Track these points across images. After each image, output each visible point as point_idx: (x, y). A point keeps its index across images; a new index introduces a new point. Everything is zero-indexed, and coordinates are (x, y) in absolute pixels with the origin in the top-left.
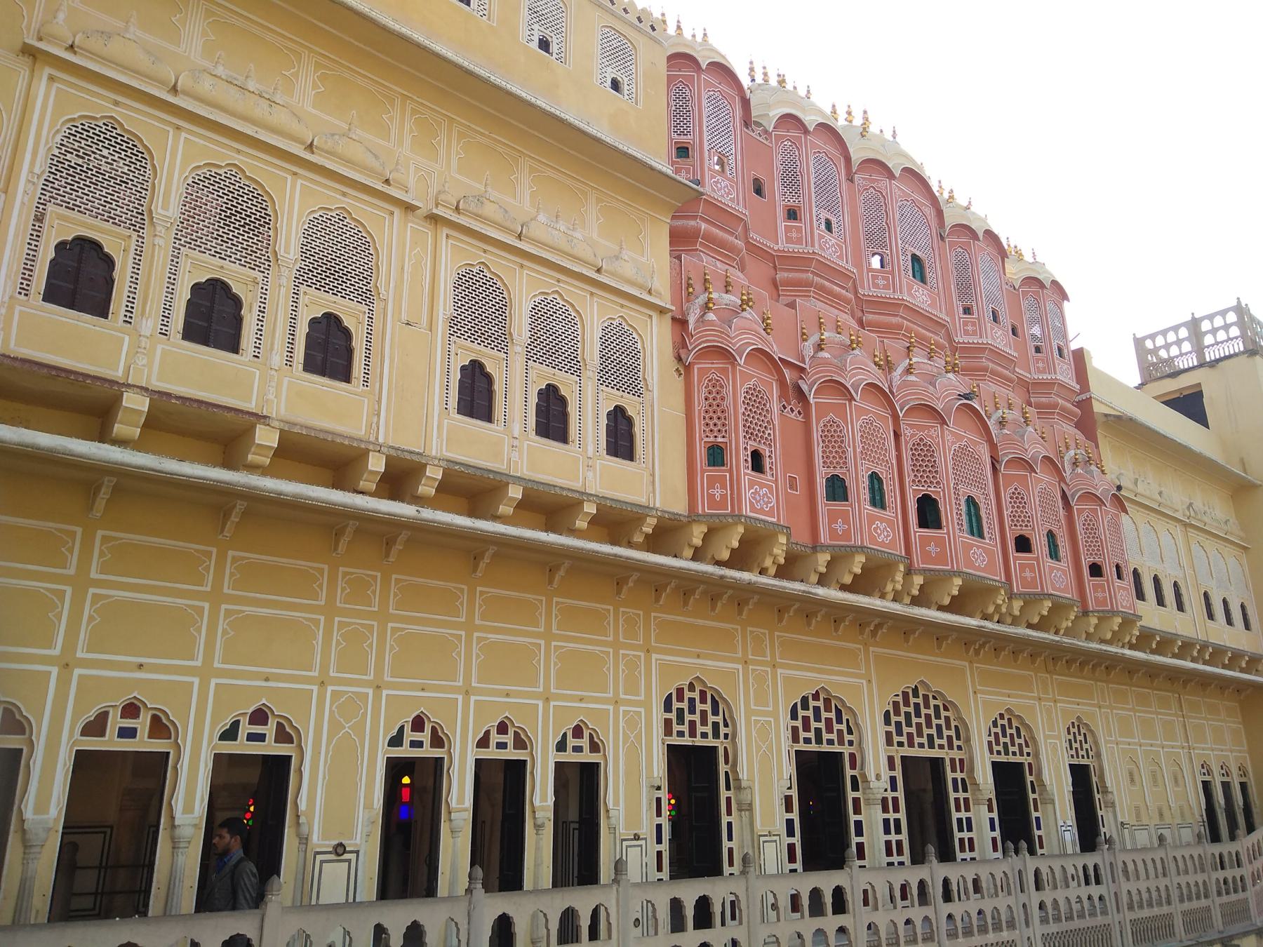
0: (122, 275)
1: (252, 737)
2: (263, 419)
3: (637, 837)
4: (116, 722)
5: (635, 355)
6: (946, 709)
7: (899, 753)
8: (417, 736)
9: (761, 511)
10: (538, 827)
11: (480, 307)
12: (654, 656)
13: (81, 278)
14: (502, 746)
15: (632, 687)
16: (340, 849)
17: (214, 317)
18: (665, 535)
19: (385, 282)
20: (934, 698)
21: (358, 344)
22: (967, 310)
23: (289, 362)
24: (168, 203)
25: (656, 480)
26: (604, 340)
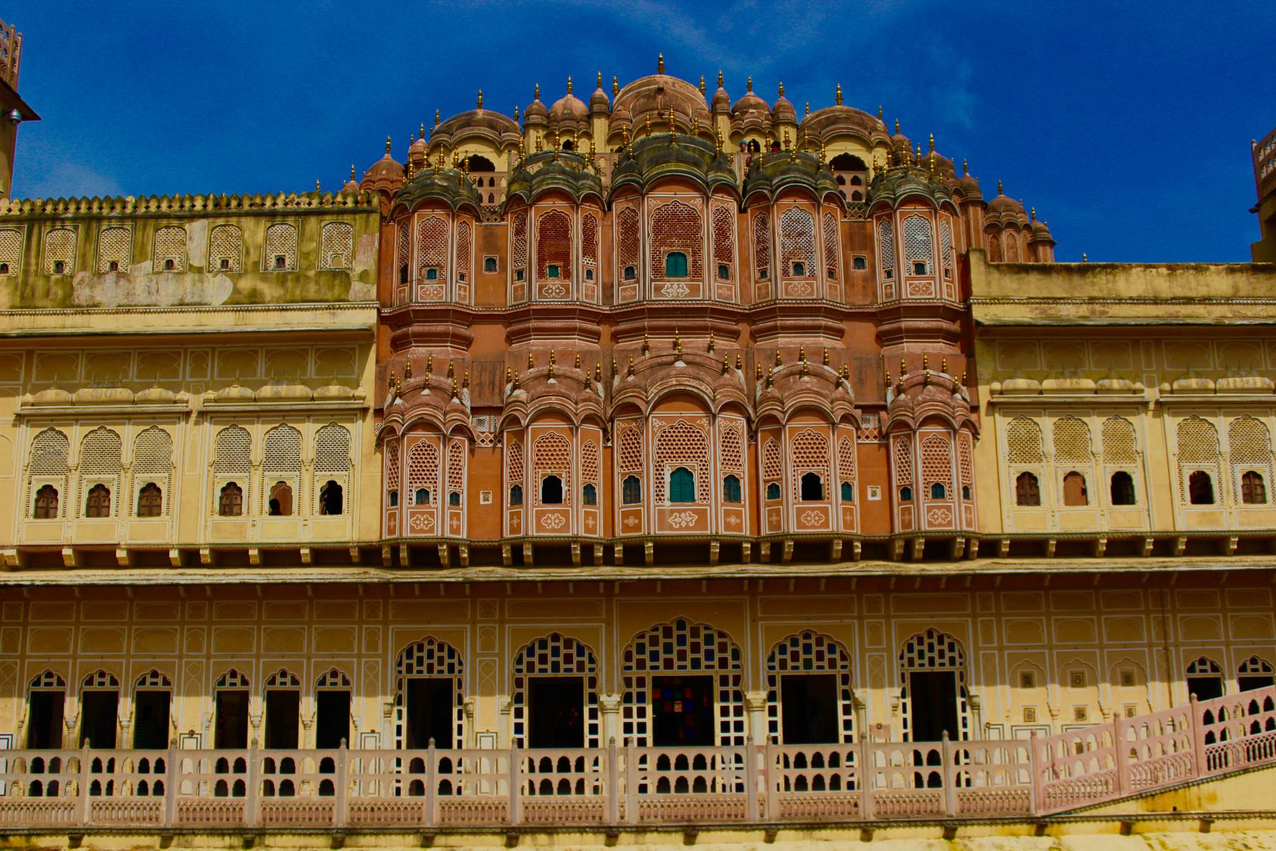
0: (60, 497)
1: (152, 684)
2: (117, 545)
4: (97, 679)
6: (721, 635)
7: (648, 674)
8: (233, 680)
9: (422, 531)
10: (305, 726)
13: (46, 502)
14: (284, 683)
15: (372, 646)
16: (192, 733)
17: (98, 501)
18: (369, 555)
19: (173, 459)
20: (707, 628)
22: (763, 274)
23: (130, 515)
25: (359, 523)
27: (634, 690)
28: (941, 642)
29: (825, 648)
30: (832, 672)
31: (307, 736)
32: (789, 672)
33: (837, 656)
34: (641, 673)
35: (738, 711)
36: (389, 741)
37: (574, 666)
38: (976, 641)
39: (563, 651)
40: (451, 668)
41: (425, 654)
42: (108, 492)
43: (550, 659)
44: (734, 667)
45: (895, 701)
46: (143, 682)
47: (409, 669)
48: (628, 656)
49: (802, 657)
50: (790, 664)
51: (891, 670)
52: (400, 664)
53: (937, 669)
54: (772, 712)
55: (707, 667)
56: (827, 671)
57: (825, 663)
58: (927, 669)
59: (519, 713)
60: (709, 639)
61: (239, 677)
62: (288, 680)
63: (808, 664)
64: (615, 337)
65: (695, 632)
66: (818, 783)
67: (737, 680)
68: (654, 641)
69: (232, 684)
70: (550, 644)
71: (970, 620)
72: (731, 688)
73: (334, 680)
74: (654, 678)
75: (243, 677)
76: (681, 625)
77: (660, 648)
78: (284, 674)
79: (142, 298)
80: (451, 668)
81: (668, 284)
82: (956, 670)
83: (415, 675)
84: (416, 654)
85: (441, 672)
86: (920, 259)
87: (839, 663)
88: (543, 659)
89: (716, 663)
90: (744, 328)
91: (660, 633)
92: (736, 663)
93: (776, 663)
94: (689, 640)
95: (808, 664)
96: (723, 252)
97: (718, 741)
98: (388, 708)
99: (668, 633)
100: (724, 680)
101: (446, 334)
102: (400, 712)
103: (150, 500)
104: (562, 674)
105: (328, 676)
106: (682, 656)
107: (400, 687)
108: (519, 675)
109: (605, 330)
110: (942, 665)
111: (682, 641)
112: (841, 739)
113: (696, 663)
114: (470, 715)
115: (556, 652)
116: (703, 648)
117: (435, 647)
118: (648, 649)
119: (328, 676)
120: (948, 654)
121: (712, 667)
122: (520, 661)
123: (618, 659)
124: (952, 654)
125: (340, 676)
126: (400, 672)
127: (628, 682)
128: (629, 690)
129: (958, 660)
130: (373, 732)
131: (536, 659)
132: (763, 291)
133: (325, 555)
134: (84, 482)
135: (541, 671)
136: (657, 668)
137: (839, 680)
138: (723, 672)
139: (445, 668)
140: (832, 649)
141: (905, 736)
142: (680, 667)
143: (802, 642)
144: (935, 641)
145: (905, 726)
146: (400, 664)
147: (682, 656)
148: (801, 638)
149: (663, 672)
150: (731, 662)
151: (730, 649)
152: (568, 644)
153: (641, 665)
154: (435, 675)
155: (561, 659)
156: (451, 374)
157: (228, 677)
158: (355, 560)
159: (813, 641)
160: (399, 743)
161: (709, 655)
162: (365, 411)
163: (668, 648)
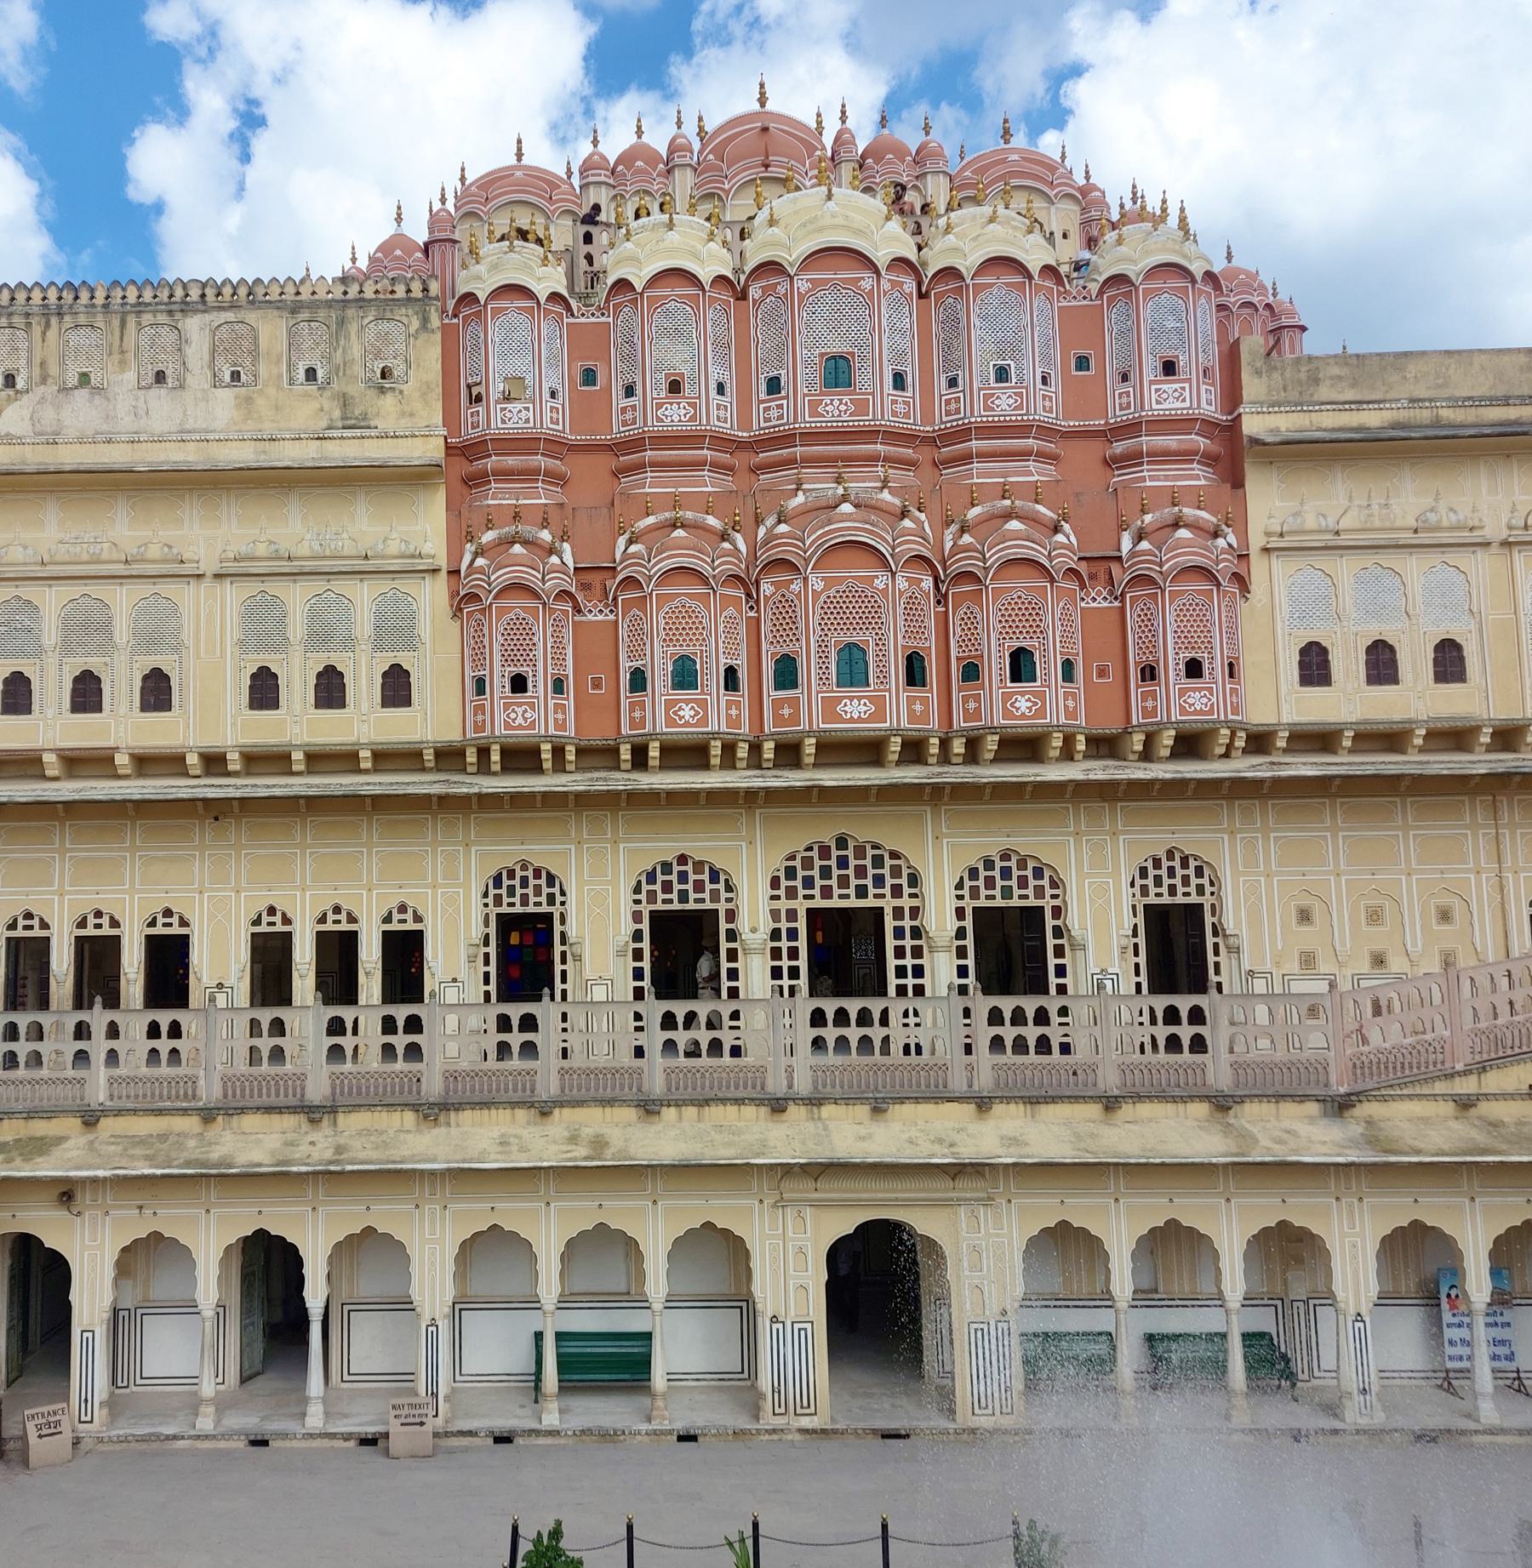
0: (35, 686)
1: (165, 925)
3: (454, 980)
4: (91, 921)
5: (413, 616)
7: (801, 906)
8: (272, 919)
10: (367, 974)
11: (262, 624)
12: (473, 849)
16: (220, 986)
17: (86, 693)
19: (184, 636)
21: (174, 683)
22: (953, 382)
24: (50, 635)
26: (379, 615)
27: (784, 925)
28: (1185, 865)
29: (1029, 873)
30: (1039, 903)
31: (370, 984)
32: (982, 903)
33: (1045, 882)
34: (792, 904)
35: (917, 952)
36: (475, 991)
37: (706, 895)
38: (1234, 862)
39: (692, 877)
40: (551, 899)
41: (517, 883)
42: (98, 680)
43: (676, 887)
44: (911, 896)
45: (1124, 942)
46: (153, 924)
47: (498, 900)
48: (775, 882)
49: (999, 883)
50: (983, 892)
51: (1118, 902)
52: (486, 895)
53: (1180, 899)
54: (961, 952)
55: (876, 896)
56: (1032, 902)
57: (1030, 892)
58: (1166, 900)
59: (638, 955)
60: (878, 861)
61: (279, 914)
62: (343, 917)
63: (1007, 893)
64: (755, 470)
65: (860, 852)
66: (1020, 1045)
67: (915, 912)
68: (808, 863)
69: (270, 924)
70: (676, 868)
71: (1226, 837)
72: (907, 923)
73: (402, 916)
74: (808, 910)
75: (284, 915)
76: (842, 842)
77: (816, 873)
78: (337, 910)
79: (126, 422)
80: (551, 899)
81: (827, 399)
82: (1206, 901)
83: (505, 909)
84: (506, 882)
85: (540, 904)
86: (1169, 354)
87: (1048, 892)
88: (667, 887)
89: (887, 891)
90: (923, 455)
91: (815, 854)
92: (913, 891)
93: (966, 892)
94: (852, 862)
95: (1007, 893)
96: (900, 355)
97: (892, 991)
98: (473, 950)
99: (825, 852)
100: (898, 913)
101: (537, 472)
102: (487, 955)
103: (157, 692)
104: (691, 906)
105: (395, 912)
106: (844, 882)
107: (487, 924)
108: (637, 907)
109: (739, 460)
110: (1185, 894)
111: (843, 863)
112: (1053, 990)
113: (862, 892)
114: (578, 958)
115: (683, 878)
116: (871, 872)
117: (530, 873)
118: (800, 873)
119: (395, 912)
120: (1194, 881)
121: (883, 896)
122: (637, 890)
123: (764, 890)
124: (1200, 881)
125: (410, 911)
126: (486, 905)
127: (775, 915)
128: (777, 925)
129: (1208, 889)
130: (454, 980)
131: (658, 887)
132: (953, 406)
133: (386, 758)
134: (66, 668)
135: (664, 901)
136: (812, 897)
137: (1048, 914)
138: (897, 902)
139: (543, 899)
140: (1038, 873)
141: (1138, 985)
142: (841, 897)
143: (998, 864)
144: (1177, 863)
145: (1137, 974)
146: (486, 895)
147: (844, 882)
148: (997, 860)
149: (819, 903)
150: (906, 890)
151: (905, 872)
152: (699, 866)
153: (791, 893)
154: (531, 909)
155: (690, 887)
156: (545, 524)
157: (264, 915)
158: (428, 765)
159: (1013, 863)
160: (487, 995)
161: (879, 881)
162: (435, 571)
163: (826, 873)
